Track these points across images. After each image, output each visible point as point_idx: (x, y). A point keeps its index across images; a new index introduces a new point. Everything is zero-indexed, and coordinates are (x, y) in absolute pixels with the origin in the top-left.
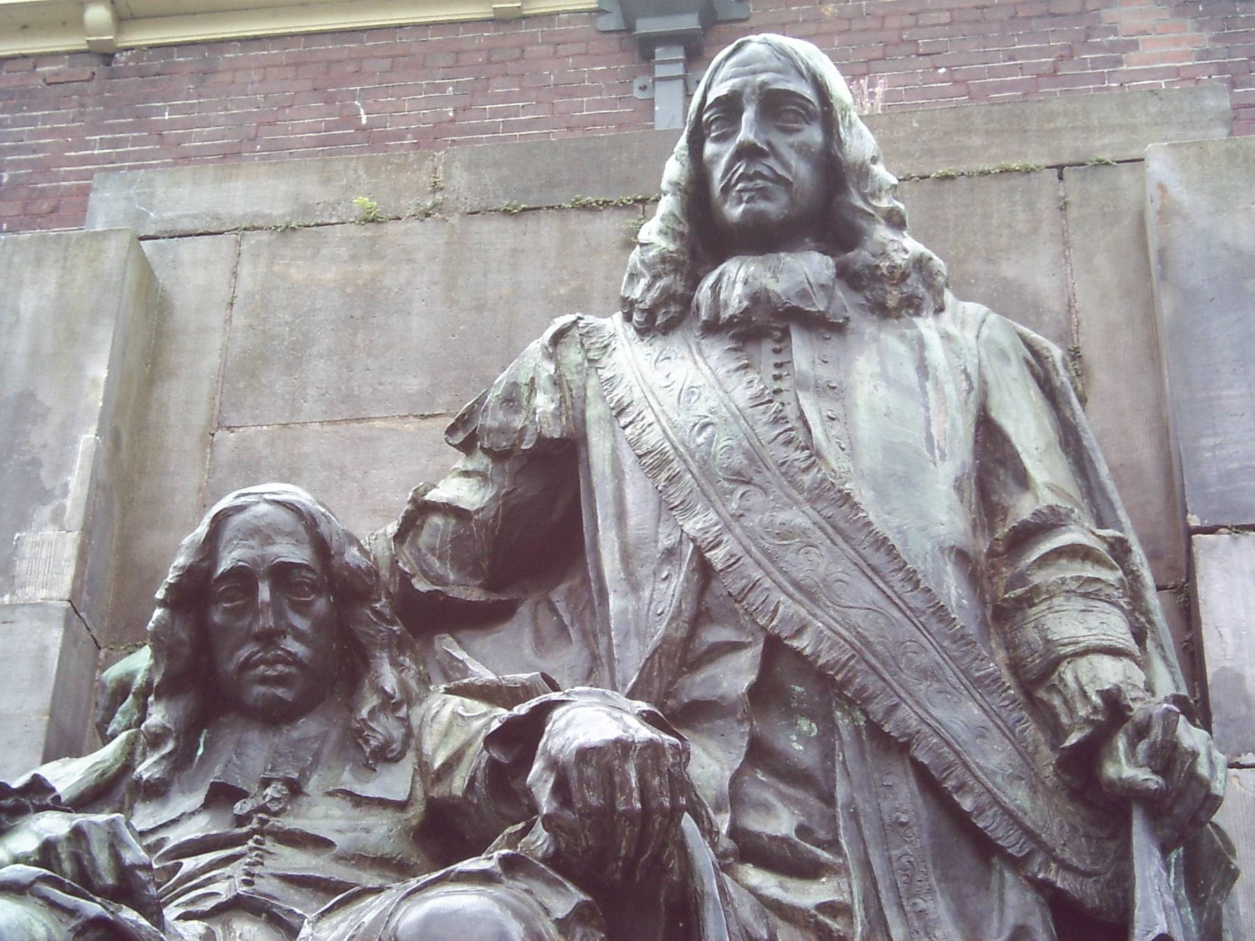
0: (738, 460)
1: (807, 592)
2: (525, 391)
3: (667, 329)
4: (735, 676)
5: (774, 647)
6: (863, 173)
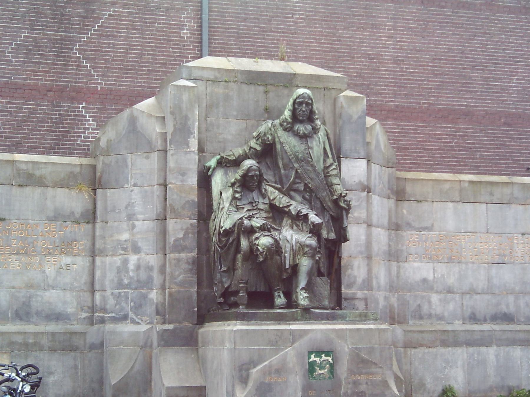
0: (302, 159)
1: (311, 179)
3: (288, 131)
5: (306, 185)
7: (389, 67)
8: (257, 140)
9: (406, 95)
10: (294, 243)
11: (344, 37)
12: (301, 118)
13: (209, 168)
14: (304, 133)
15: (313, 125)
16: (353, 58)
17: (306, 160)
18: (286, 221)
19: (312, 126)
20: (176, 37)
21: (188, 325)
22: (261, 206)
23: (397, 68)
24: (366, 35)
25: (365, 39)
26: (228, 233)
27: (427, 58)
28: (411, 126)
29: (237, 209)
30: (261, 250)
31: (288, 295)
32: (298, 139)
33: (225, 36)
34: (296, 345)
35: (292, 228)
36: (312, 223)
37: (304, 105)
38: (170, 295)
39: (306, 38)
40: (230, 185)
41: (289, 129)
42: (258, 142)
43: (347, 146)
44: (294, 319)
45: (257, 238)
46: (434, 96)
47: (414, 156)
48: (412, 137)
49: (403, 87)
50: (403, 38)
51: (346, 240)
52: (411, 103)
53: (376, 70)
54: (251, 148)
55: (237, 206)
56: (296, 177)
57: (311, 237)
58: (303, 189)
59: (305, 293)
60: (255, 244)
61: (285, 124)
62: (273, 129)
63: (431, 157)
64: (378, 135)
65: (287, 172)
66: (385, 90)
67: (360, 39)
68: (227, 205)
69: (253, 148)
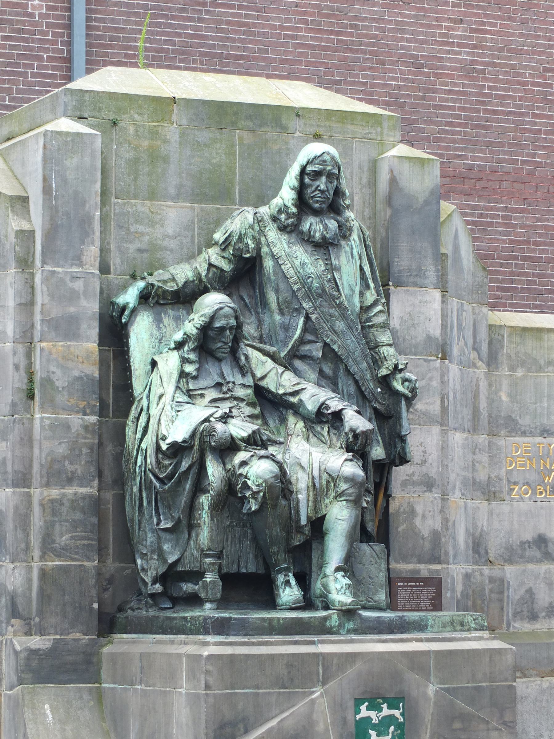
0: (320, 291)
2: (243, 236)
4: (316, 350)
6: (344, 194)
7: (455, 84)
8: (223, 250)
9: (489, 144)
10: (316, 474)
11: (364, 19)
12: (317, 205)
13: (124, 309)
14: (324, 238)
15: (340, 219)
16: (383, 63)
17: (327, 294)
18: (295, 425)
19: (338, 222)
20: (18, 14)
21: (81, 638)
22: (240, 392)
23: (470, 86)
24: (409, 16)
25: (408, 24)
26: (177, 450)
27: (533, 68)
28: (498, 209)
29: (190, 396)
30: (255, 488)
31: (304, 581)
32: (310, 249)
33: (120, 13)
34: (332, 684)
35: (308, 439)
36: (352, 430)
37: (324, 179)
38: (43, 574)
39: (288, 20)
40: (173, 346)
41: (290, 229)
42: (226, 255)
43: (402, 262)
44: (322, 629)
45: (244, 463)
46: (545, 148)
47: (503, 273)
48: (500, 233)
49: (484, 127)
50: (483, 24)
51: (403, 460)
52: (499, 161)
53: (428, 90)
54: (211, 265)
55: (189, 391)
56: (305, 330)
57: (351, 460)
58: (320, 355)
59: (344, 577)
60: (241, 475)
61: (283, 217)
62: (256, 227)
63: (539, 276)
64: (456, 237)
65: (287, 318)
66: (446, 132)
67: (397, 23)
68: (170, 388)
69: (215, 266)
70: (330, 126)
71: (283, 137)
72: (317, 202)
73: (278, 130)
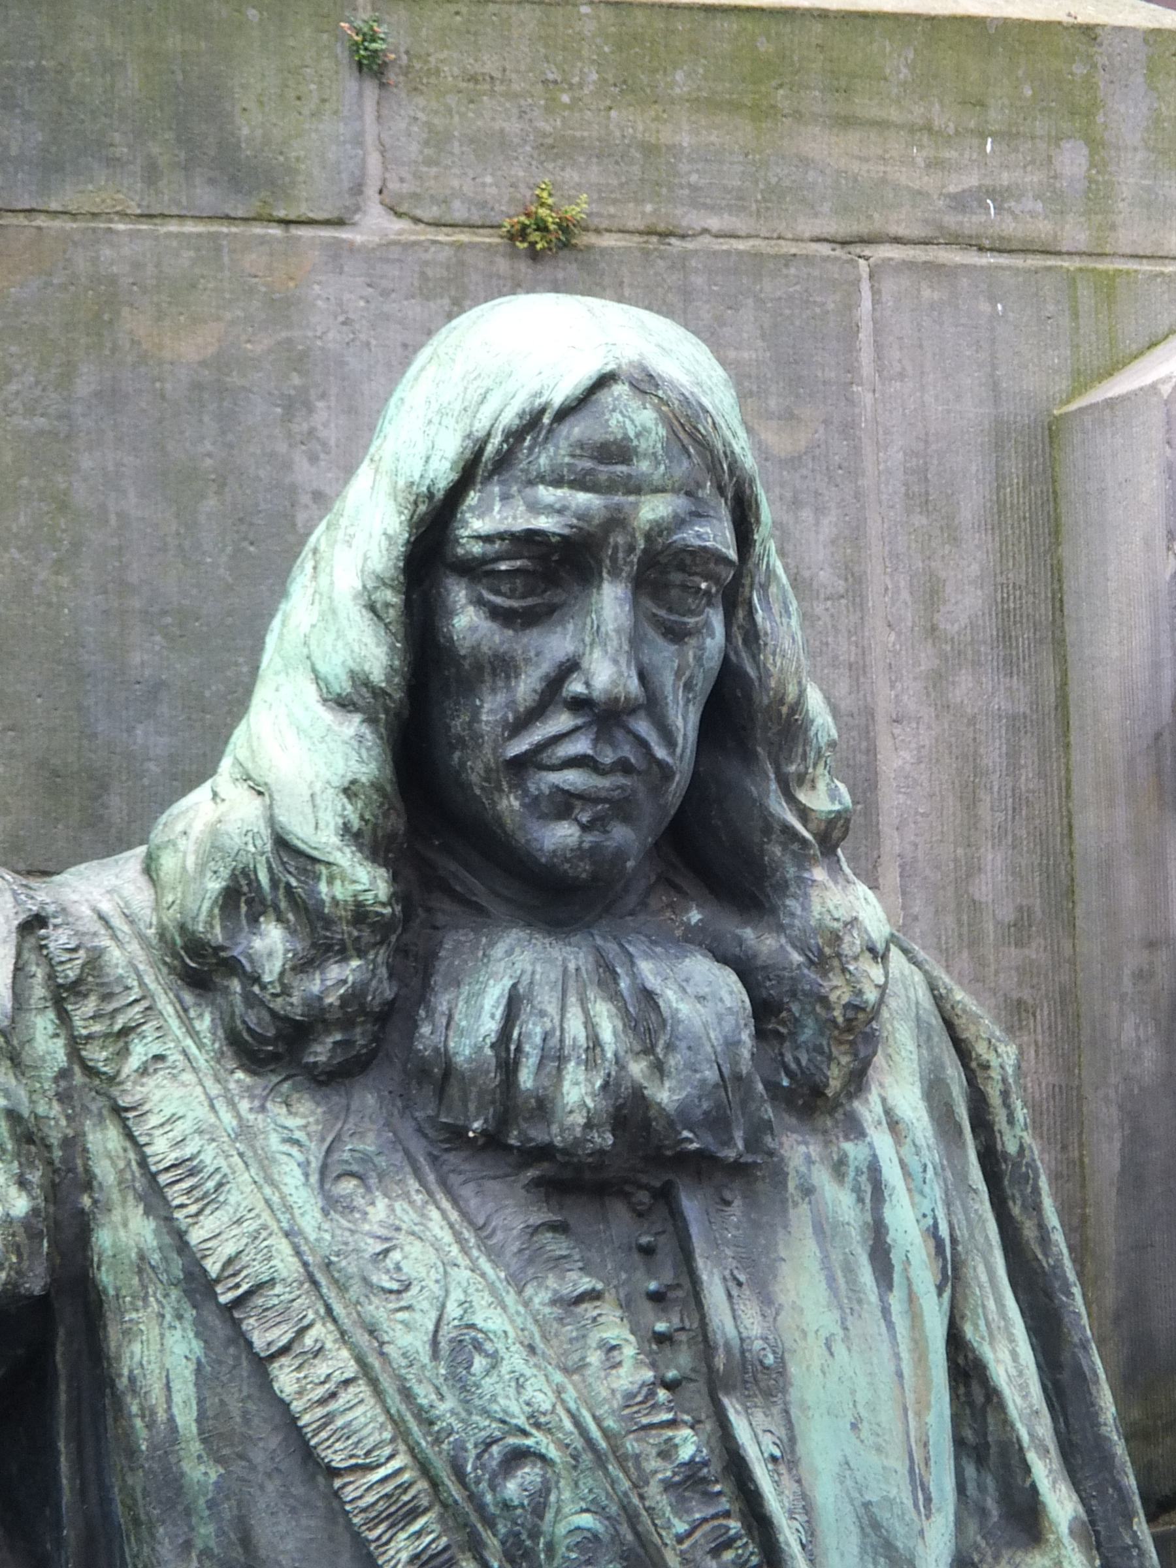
12: (561, 835)
70: (650, 150)
71: (252, 260)
72: (563, 805)
73: (206, 196)
